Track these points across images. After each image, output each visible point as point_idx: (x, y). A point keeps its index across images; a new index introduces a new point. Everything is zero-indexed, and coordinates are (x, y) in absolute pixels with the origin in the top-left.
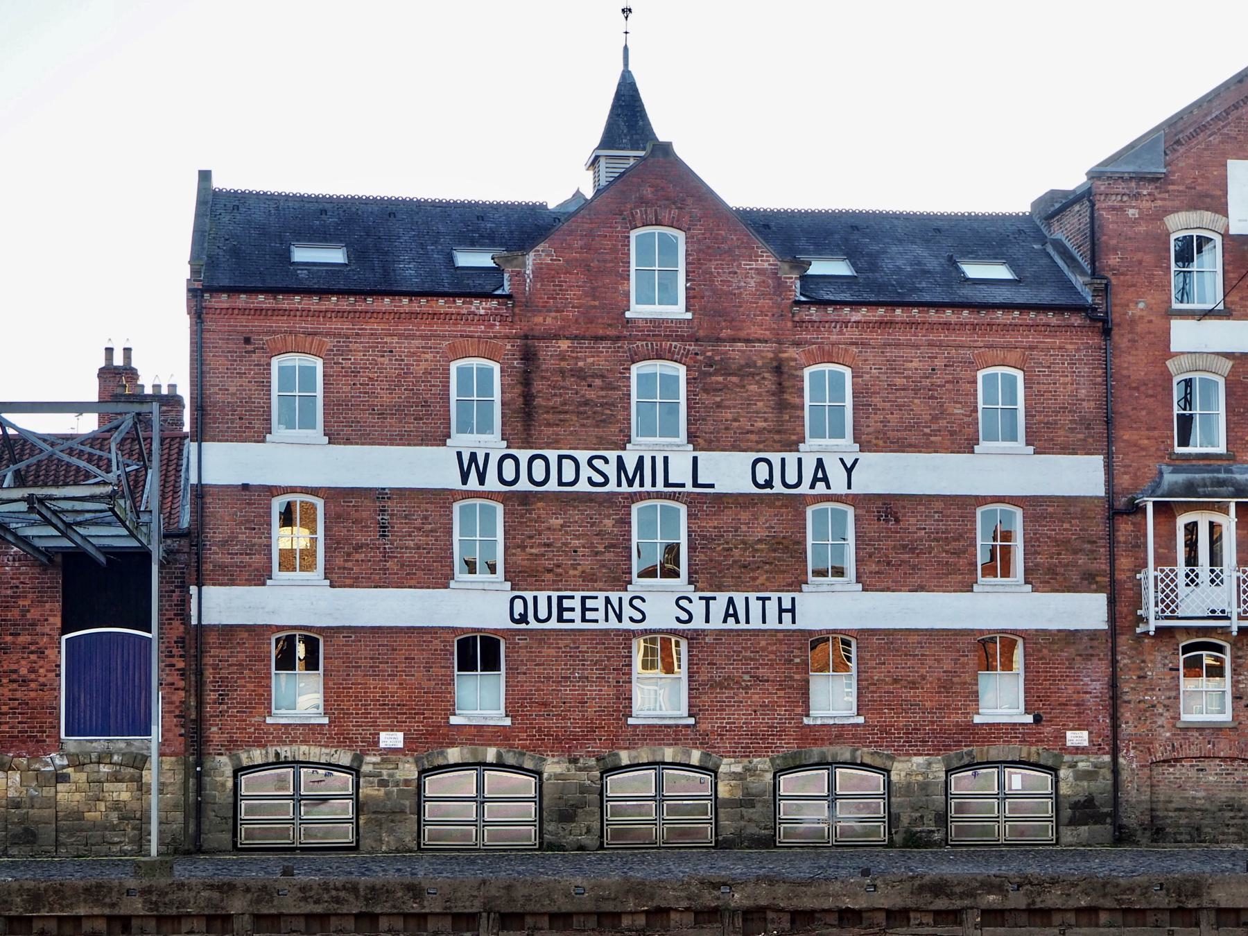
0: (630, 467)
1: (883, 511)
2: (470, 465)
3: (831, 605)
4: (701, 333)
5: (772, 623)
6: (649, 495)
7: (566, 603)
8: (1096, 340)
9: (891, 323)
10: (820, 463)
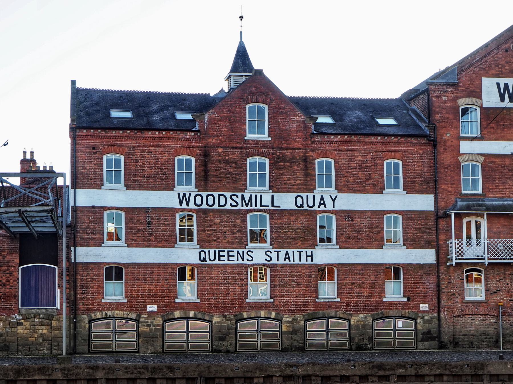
0: (247, 199)
1: (347, 216)
2: (183, 198)
3: (326, 255)
4: (275, 146)
5: (303, 261)
6: (254, 210)
7: (222, 253)
8: (430, 149)
10: (322, 198)
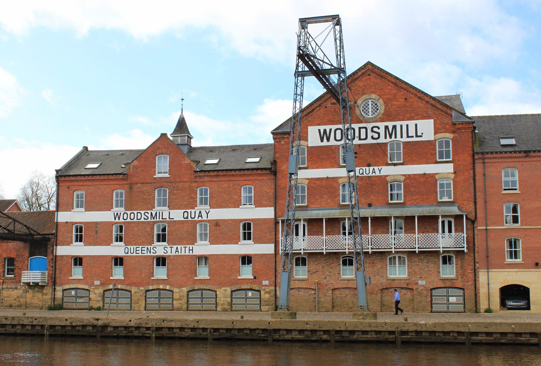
0: (154, 215)
1: (217, 223)
2: (117, 216)
3: (203, 248)
4: (172, 180)
5: (187, 253)
6: (158, 222)
7: (137, 249)
8: (272, 177)
9: (218, 175)
10: (200, 212)
